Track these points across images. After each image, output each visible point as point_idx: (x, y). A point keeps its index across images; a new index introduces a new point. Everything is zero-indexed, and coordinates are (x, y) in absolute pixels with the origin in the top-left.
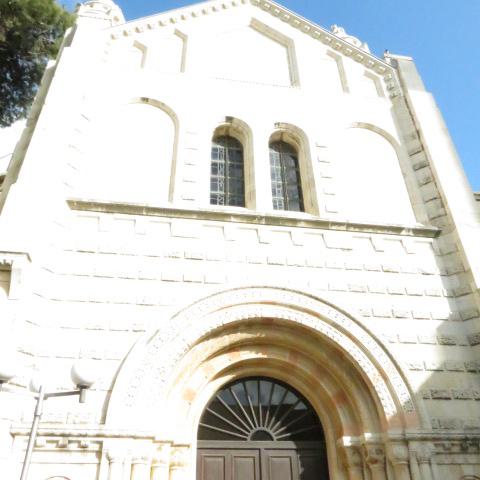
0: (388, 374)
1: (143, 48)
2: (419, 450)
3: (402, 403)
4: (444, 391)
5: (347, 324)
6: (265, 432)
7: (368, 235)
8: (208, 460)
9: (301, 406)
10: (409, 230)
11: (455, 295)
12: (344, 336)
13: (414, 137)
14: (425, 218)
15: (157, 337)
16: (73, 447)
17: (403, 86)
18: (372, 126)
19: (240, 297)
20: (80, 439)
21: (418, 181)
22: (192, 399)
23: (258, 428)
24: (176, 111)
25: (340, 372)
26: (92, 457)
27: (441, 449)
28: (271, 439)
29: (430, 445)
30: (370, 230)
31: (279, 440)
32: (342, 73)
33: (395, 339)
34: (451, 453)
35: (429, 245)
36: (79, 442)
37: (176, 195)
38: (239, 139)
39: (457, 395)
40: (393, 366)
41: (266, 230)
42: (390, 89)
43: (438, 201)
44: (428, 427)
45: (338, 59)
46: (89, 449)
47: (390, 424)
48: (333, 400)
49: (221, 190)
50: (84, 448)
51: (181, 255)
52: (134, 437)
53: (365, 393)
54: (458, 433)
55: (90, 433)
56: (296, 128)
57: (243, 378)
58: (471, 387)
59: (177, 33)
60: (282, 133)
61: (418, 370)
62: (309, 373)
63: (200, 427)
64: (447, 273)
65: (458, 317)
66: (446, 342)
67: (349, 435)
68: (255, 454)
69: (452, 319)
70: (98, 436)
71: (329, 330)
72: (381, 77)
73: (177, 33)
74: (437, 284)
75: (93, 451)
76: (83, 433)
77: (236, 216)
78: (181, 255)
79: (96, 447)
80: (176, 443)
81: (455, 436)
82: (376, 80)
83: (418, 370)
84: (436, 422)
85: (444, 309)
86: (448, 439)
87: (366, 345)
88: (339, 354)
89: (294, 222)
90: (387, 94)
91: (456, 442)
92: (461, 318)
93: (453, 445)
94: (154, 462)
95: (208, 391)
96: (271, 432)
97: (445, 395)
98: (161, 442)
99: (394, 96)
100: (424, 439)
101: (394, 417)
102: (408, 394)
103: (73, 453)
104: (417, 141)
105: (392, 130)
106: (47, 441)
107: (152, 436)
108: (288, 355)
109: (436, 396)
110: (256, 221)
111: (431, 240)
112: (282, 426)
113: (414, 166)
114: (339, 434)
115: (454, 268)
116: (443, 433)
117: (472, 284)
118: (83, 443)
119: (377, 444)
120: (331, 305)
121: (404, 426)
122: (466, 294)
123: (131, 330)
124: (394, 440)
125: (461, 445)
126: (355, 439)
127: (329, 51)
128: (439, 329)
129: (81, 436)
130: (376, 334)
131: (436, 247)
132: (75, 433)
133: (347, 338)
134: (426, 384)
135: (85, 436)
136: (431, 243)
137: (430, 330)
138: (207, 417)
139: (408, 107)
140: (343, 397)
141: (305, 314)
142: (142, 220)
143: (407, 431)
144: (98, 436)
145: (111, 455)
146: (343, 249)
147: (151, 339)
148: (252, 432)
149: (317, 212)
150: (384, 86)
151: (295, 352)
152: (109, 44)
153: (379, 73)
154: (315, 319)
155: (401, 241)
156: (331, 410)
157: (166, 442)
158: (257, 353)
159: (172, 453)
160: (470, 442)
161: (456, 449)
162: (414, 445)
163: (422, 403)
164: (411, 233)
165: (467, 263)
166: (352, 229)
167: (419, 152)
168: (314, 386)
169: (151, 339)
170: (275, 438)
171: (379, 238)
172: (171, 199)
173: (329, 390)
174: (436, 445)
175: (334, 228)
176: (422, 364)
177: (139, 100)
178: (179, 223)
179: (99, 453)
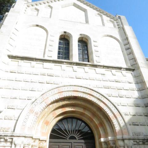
0: (117, 116)
1: (38, 10)
2: (128, 143)
3: (122, 126)
4: (137, 122)
5: (100, 97)
6: (75, 138)
7: (111, 70)
8: (53, 146)
9: (86, 129)
10: (124, 68)
11: (140, 90)
12: (102, 103)
13: (125, 40)
14: (130, 65)
15: (35, 102)
16: (2, 140)
17: (122, 24)
18: (112, 36)
19: (66, 89)
20: (5, 137)
21: (127, 54)
22: (48, 124)
23: (71, 135)
24: (47, 29)
25: (100, 116)
26: (9, 144)
27: (135, 143)
28: (76, 139)
29: (132, 141)
30: (111, 68)
31: (78, 139)
32: (102, 20)
33: (120, 105)
34: (139, 144)
35: (131, 74)
36: (4, 138)
37: (46, 55)
38: (68, 39)
39: (141, 124)
40: (119, 113)
41: (75, 67)
42: (118, 25)
43: (134, 60)
44: (131, 136)
45: (101, 16)
47: (117, 134)
48: (98, 125)
49: (61, 55)
50: (6, 141)
51: (46, 74)
52: (25, 137)
53: (109, 122)
54: (141, 137)
55: (8, 135)
56: (87, 36)
57: (66, 118)
59: (49, 6)
60: (82, 38)
61: (127, 115)
62: (90, 115)
64: (137, 83)
65: (141, 97)
66: (137, 106)
67: (103, 138)
68: (70, 144)
69: (139, 98)
70: (11, 136)
72: (115, 22)
73: (49, 6)
74: (134, 86)
75: (9, 142)
76: (6, 135)
77: (65, 62)
78: (46, 74)
79: (10, 140)
80: (41, 140)
81: (141, 138)
82: (113, 22)
83: (127, 115)
84: (134, 133)
85: (136, 94)
86: (138, 139)
87: (109, 106)
88: (100, 109)
89: (85, 65)
90: (117, 27)
92: (143, 98)
93: (140, 141)
94: (32, 146)
95: (53, 122)
96: (76, 136)
97: (137, 124)
98: (35, 139)
100: (130, 139)
101: (119, 131)
102: (124, 123)
103: (2, 143)
104: (127, 41)
105: (118, 37)
107: (31, 136)
108: (82, 109)
109: (134, 124)
110: (72, 64)
111: (132, 72)
112: (79, 135)
113: (126, 49)
114: (100, 137)
115: (140, 81)
116: (136, 137)
117: (145, 86)
118: (6, 139)
119: (113, 141)
120: (97, 92)
121: (123, 135)
122: (144, 90)
123: (27, 99)
124: (119, 139)
125: (143, 142)
126: (105, 139)
127: (98, 13)
128: (135, 101)
129: (5, 136)
130: (113, 102)
131: (133, 74)
132: (3, 135)
133: (103, 104)
134: (130, 119)
135: (7, 136)
136: (131, 73)
137: (131, 101)
138: (53, 131)
139: (124, 30)
140: (102, 124)
141: (88, 95)
142: (34, 63)
143: (124, 136)
144: (11, 136)
145: (16, 143)
146: (102, 74)
147: (34, 102)
148: (69, 136)
149: (93, 62)
150: (116, 24)
151: (85, 108)
152: (26, 8)
153: (115, 21)
154: (92, 97)
155: (121, 72)
156: (97, 128)
157: (37, 139)
158: (74, 109)
159: (40, 143)
160: (146, 140)
161: (141, 143)
162: (126, 141)
163: (129, 126)
164: (125, 70)
165: (144, 79)
166: (105, 68)
168: (92, 121)
169: (34, 102)
170: (77, 139)
171: (114, 71)
172: (44, 57)
173: (96, 122)
174: (134, 141)
175: (99, 67)
176: (129, 113)
178: (46, 64)
179: (11, 143)
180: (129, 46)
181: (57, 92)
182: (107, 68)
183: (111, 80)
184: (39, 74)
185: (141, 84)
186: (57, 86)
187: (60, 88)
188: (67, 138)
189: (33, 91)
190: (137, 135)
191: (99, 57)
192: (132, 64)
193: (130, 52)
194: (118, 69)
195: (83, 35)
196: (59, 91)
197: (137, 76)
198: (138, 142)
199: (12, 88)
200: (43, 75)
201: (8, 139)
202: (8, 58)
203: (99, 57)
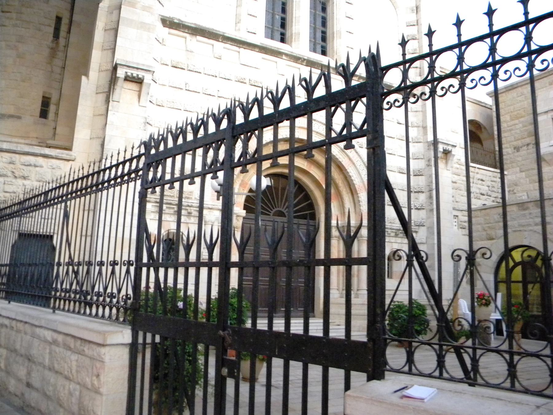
6: (284, 213)
20: (188, 208)
43: (418, 70)
46: (193, 215)
51: (247, 81)
63: (245, 205)
71: (338, 154)
76: (190, 204)
78: (247, 81)
81: (395, 228)
86: (391, 229)
91: (394, 231)
106: (167, 207)
118: (189, 211)
129: (188, 206)
142: (219, 46)
161: (393, 234)
167: (414, 25)
178: (246, 53)
185: (418, 130)
188: (270, 212)
190: (390, 223)
193: (415, 50)
197: (416, 110)
198: (389, 232)
199: (183, 110)
200: (241, 82)
201: (192, 211)
202: (160, 25)
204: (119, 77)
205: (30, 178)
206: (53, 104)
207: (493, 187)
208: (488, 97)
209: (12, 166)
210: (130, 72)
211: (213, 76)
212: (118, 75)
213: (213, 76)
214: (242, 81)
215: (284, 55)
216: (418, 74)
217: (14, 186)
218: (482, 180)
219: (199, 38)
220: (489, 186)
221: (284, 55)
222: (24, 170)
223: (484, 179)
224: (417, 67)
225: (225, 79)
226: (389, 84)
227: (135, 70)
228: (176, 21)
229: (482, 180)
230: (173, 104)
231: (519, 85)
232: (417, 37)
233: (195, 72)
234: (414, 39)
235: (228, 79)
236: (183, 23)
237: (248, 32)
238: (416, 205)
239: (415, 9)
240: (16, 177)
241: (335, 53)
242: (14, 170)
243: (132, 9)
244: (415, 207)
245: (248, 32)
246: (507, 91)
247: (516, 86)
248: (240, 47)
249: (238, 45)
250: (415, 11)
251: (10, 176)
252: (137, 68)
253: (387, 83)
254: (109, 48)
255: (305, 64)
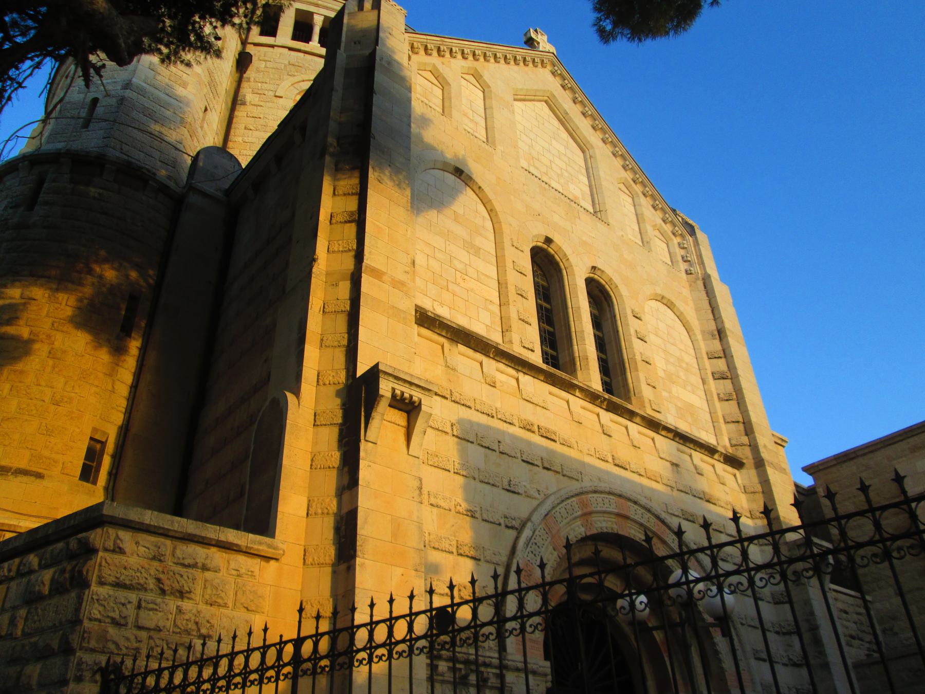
10: (722, 453)
18: (675, 306)
21: (718, 395)
30: (692, 446)
56: (611, 279)
58: (778, 649)
72: (676, 240)
99: (691, 274)
142: (492, 366)
150: (680, 253)
153: (674, 234)
166: (677, 439)
167: (720, 357)
175: (663, 433)
177: (451, 170)
180: (725, 368)
181: (580, 513)
182: (681, 441)
183: (695, 494)
184: (516, 422)
186: (575, 487)
187: (583, 496)
189: (514, 492)
191: (654, 387)
192: (734, 442)
193: (730, 394)
194: (706, 453)
195: (598, 273)
196: (585, 510)
203: (654, 387)
204: (382, 396)
205: (192, 595)
206: (108, 454)
207: (862, 624)
208: (805, 474)
209: (156, 564)
210: (400, 388)
211: (489, 415)
212: (381, 392)
213: (489, 415)
214: (528, 427)
215: (577, 390)
216: (743, 432)
217: (160, 614)
218: (846, 612)
219: (461, 348)
220: (855, 623)
221: (577, 390)
222: (182, 576)
223: (847, 609)
224: (738, 422)
225: (505, 422)
226: (712, 446)
227: (407, 385)
228: (430, 314)
229: (846, 612)
230: (437, 458)
231: (859, 453)
232: (728, 374)
233: (463, 405)
234: (724, 378)
235: (510, 423)
236: (441, 319)
237: (524, 347)
238: (791, 657)
239: (716, 333)
240: (163, 592)
241: (633, 393)
242: (162, 576)
243: (376, 281)
244: (791, 662)
245: (524, 347)
246: (838, 464)
247: (853, 455)
248: (518, 371)
249: (516, 367)
250: (717, 336)
251: (152, 590)
252: (411, 384)
253: (709, 445)
254: (336, 344)
255: (605, 407)
